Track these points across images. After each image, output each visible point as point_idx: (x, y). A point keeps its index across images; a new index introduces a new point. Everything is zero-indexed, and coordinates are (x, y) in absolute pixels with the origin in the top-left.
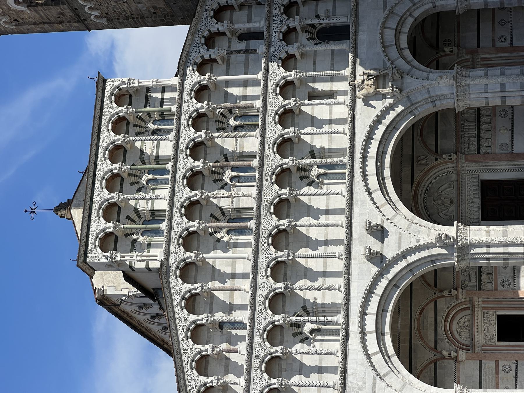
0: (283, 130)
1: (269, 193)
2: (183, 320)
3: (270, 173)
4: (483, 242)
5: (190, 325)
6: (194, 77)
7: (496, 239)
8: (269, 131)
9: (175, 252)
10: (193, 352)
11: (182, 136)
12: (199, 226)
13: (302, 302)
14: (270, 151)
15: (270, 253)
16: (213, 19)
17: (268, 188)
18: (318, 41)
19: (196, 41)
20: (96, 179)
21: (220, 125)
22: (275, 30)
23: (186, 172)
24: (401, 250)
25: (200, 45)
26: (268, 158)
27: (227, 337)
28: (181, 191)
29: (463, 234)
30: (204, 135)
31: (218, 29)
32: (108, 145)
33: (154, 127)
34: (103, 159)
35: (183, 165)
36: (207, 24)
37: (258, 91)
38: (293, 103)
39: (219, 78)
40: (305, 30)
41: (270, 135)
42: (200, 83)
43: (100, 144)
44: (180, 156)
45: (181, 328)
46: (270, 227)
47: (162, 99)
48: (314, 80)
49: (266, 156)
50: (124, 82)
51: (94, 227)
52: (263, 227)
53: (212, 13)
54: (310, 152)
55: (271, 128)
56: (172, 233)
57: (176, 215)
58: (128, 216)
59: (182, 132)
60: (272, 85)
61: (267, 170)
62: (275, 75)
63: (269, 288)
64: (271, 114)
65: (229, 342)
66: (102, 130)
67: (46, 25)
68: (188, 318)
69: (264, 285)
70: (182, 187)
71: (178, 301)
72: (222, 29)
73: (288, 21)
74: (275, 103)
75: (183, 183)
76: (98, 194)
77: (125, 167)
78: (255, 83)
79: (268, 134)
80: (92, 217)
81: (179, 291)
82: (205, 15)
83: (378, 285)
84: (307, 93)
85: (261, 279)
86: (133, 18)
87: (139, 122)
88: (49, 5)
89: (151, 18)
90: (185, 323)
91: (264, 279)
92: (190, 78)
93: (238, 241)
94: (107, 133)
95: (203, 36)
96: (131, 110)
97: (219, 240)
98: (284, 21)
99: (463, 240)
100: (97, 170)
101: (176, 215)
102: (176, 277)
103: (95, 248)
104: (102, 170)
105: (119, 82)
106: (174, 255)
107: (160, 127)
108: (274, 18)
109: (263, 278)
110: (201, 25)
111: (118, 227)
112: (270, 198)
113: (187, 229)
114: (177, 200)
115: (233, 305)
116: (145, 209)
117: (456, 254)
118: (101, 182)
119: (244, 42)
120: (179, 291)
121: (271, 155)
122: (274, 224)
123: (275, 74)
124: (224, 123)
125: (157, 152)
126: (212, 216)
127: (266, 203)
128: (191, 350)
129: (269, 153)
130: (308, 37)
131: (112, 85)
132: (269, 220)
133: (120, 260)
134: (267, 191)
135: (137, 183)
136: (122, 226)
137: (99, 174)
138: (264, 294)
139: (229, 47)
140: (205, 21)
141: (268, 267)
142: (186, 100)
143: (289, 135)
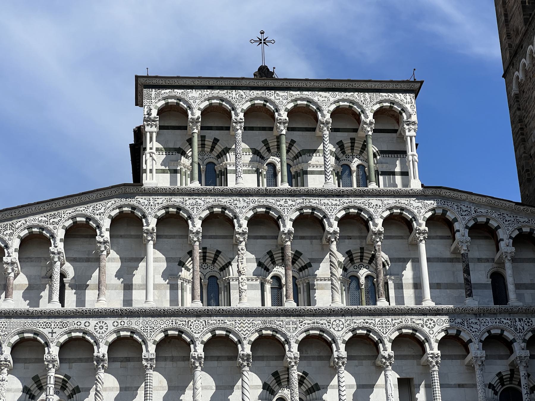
0: (344, 342)
1: (244, 326)
2: (56, 220)
3: (274, 326)
5: (49, 231)
6: (422, 211)
8: (340, 321)
9: (156, 202)
10: (8, 237)
11: (331, 201)
12: (194, 233)
13: (86, 386)
14: (308, 324)
15: (153, 333)
16: (517, 232)
17: (251, 324)
18: (499, 389)
19: (479, 210)
20: (263, 91)
21: (356, 255)
22: (505, 321)
23: (275, 210)
25: (474, 215)
26: (298, 323)
27: (37, 285)
28: (246, 205)
30: (331, 230)
31: (502, 240)
32: (315, 103)
33: (354, 167)
34: (293, 98)
35: (286, 205)
36: (507, 223)
37: (409, 302)
38: (386, 354)
39: (423, 246)
40: (514, 371)
41: (334, 323)
42: (413, 220)
43: (317, 92)
44: (299, 200)
45: (44, 219)
46: (192, 331)
47: (393, 173)
48: (429, 387)
49: (301, 319)
50: (410, 116)
51: (194, 93)
52: (192, 321)
53: (526, 230)
54: (317, 384)
55: (346, 324)
56: (183, 197)
57: (211, 201)
58: (218, 140)
59: (336, 200)
60: (414, 322)
61: (279, 322)
62: (431, 326)
63: (98, 335)
64: (367, 323)
65: (30, 288)
66: (337, 93)
67: (503, 18)
68: (57, 226)
69: (104, 329)
70: (252, 205)
71: (83, 212)
72: (502, 244)
73: (521, 341)
74: (386, 327)
75: (260, 207)
76: (242, 95)
77: (282, 128)
78: (419, 299)
79: (335, 321)
80: (209, 90)
81: (98, 212)
82: (522, 220)
84: (411, 377)
85: (114, 322)
86: (522, 129)
87: (358, 145)
88: (523, 11)
89: (524, 152)
90: (52, 224)
91: (113, 328)
92: (420, 205)
93: (180, 291)
94: (332, 100)
95: (488, 220)
96: (369, 129)
97: (182, 264)
98: (521, 334)
100: (277, 92)
101: (211, 201)
102: (120, 207)
103: (164, 99)
104: (277, 98)
105: (410, 110)
106: (151, 202)
107: (354, 174)
108: (524, 319)
109: (114, 326)
110: (505, 215)
111: (194, 125)
112: (236, 329)
113: (190, 217)
114: (232, 201)
115: (85, 289)
116: (229, 161)
118: (260, 98)
119: (489, 281)
120: (98, 212)
121: (302, 327)
122: (196, 336)
123: (432, 325)
124: (361, 261)
125: (313, 173)
126: (218, 253)
127: (228, 323)
128: (11, 234)
129: (305, 324)
130: (503, 374)
131: (405, 101)
132: (203, 328)
133: (147, 132)
134: (247, 324)
135: (268, 150)
136: (196, 131)
137: (271, 95)
138: (91, 329)
139: (480, 260)
140: (513, 220)
141: (132, 332)
142: (385, 202)
143: (336, 351)
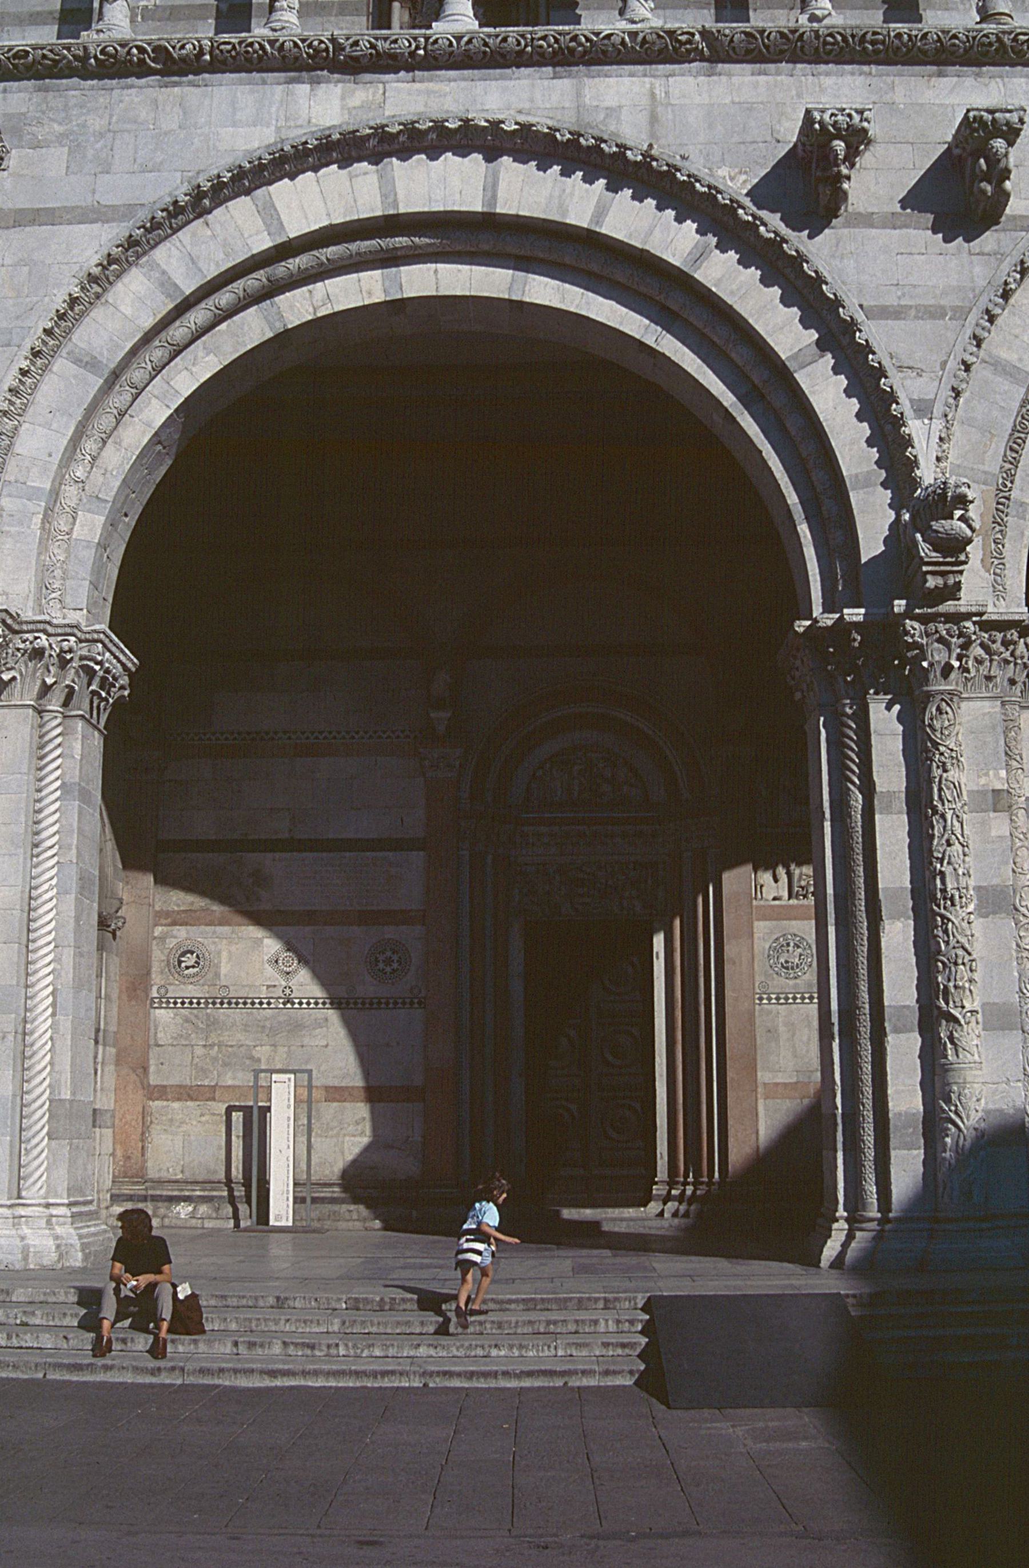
4: (937, 772)
7: (957, 847)
24: (860, 317)
29: (979, 661)
83: (660, 208)
99: (938, 654)
117: (855, 614)
